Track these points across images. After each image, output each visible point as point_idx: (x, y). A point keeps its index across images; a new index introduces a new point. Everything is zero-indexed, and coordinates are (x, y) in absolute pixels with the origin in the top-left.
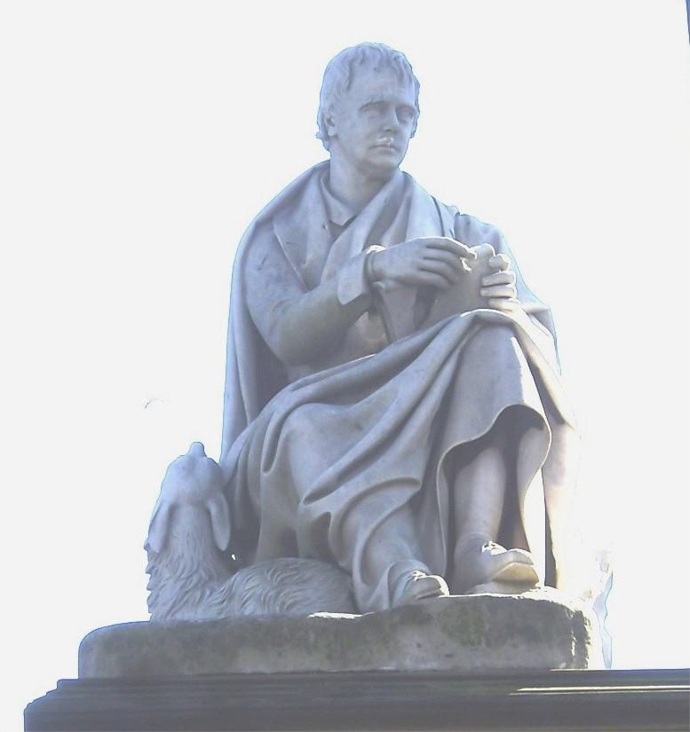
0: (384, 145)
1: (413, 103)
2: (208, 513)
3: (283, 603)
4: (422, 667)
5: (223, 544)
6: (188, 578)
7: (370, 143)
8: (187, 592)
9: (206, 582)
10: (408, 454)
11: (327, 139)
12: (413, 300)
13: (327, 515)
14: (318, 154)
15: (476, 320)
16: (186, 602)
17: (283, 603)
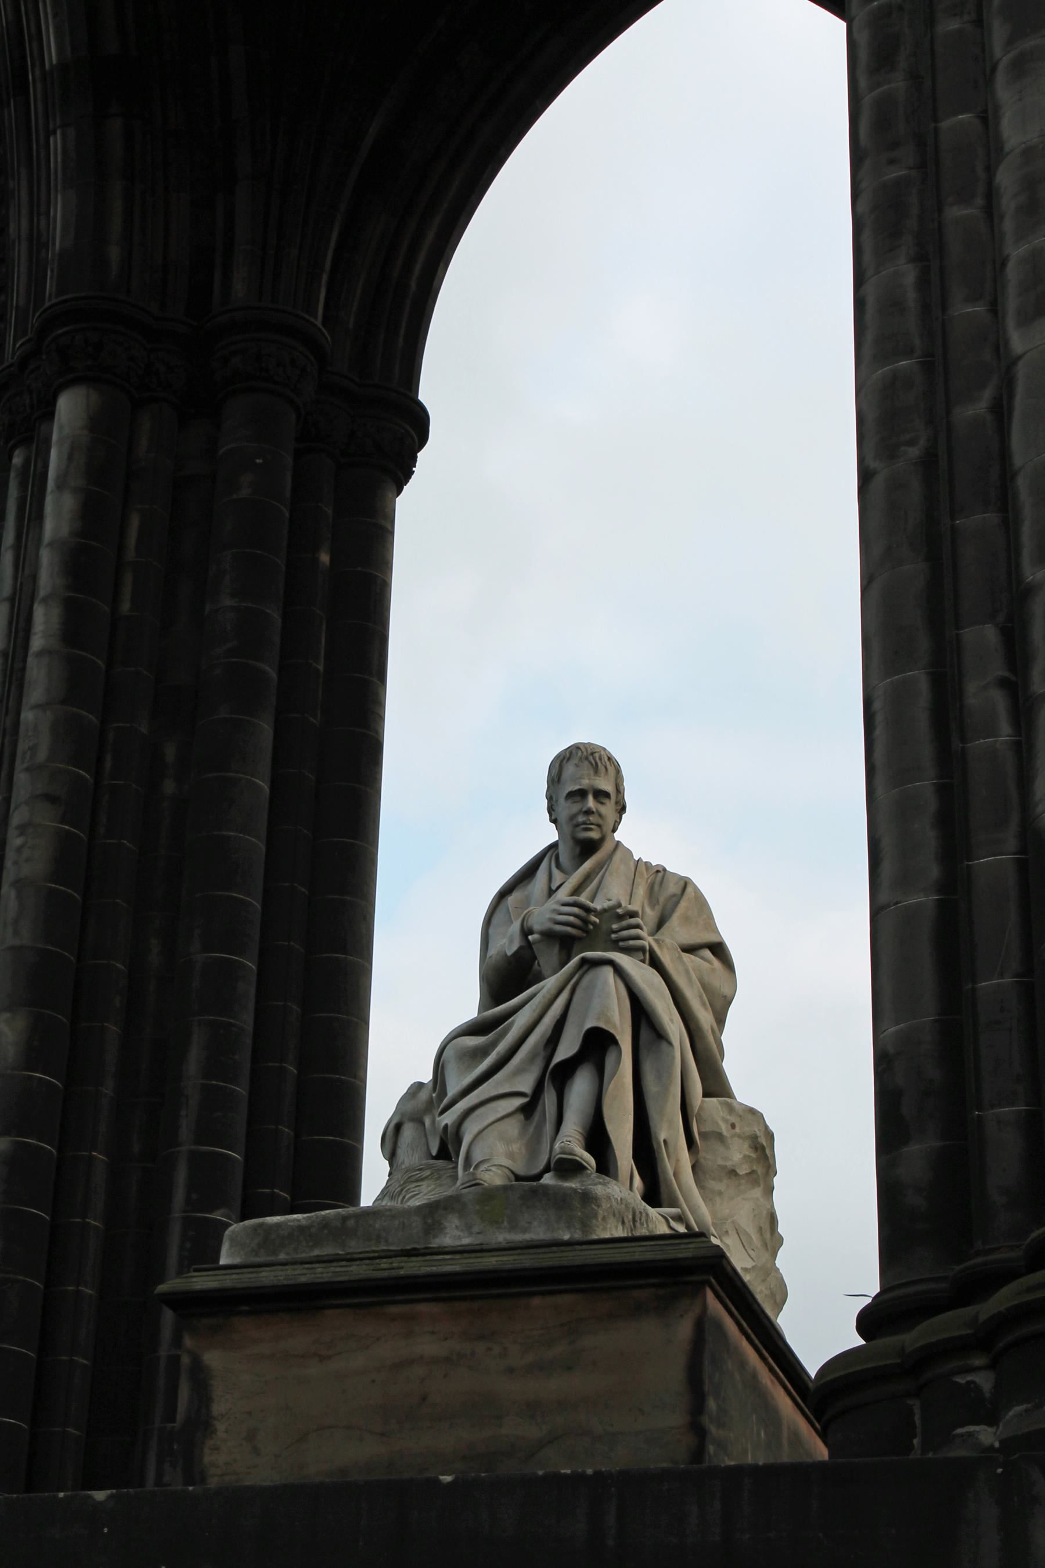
0: (584, 823)
1: (607, 786)
4: (458, 1243)
5: (434, 1152)
7: (574, 822)
11: (554, 821)
12: (556, 949)
13: (446, 1125)
14: (550, 834)
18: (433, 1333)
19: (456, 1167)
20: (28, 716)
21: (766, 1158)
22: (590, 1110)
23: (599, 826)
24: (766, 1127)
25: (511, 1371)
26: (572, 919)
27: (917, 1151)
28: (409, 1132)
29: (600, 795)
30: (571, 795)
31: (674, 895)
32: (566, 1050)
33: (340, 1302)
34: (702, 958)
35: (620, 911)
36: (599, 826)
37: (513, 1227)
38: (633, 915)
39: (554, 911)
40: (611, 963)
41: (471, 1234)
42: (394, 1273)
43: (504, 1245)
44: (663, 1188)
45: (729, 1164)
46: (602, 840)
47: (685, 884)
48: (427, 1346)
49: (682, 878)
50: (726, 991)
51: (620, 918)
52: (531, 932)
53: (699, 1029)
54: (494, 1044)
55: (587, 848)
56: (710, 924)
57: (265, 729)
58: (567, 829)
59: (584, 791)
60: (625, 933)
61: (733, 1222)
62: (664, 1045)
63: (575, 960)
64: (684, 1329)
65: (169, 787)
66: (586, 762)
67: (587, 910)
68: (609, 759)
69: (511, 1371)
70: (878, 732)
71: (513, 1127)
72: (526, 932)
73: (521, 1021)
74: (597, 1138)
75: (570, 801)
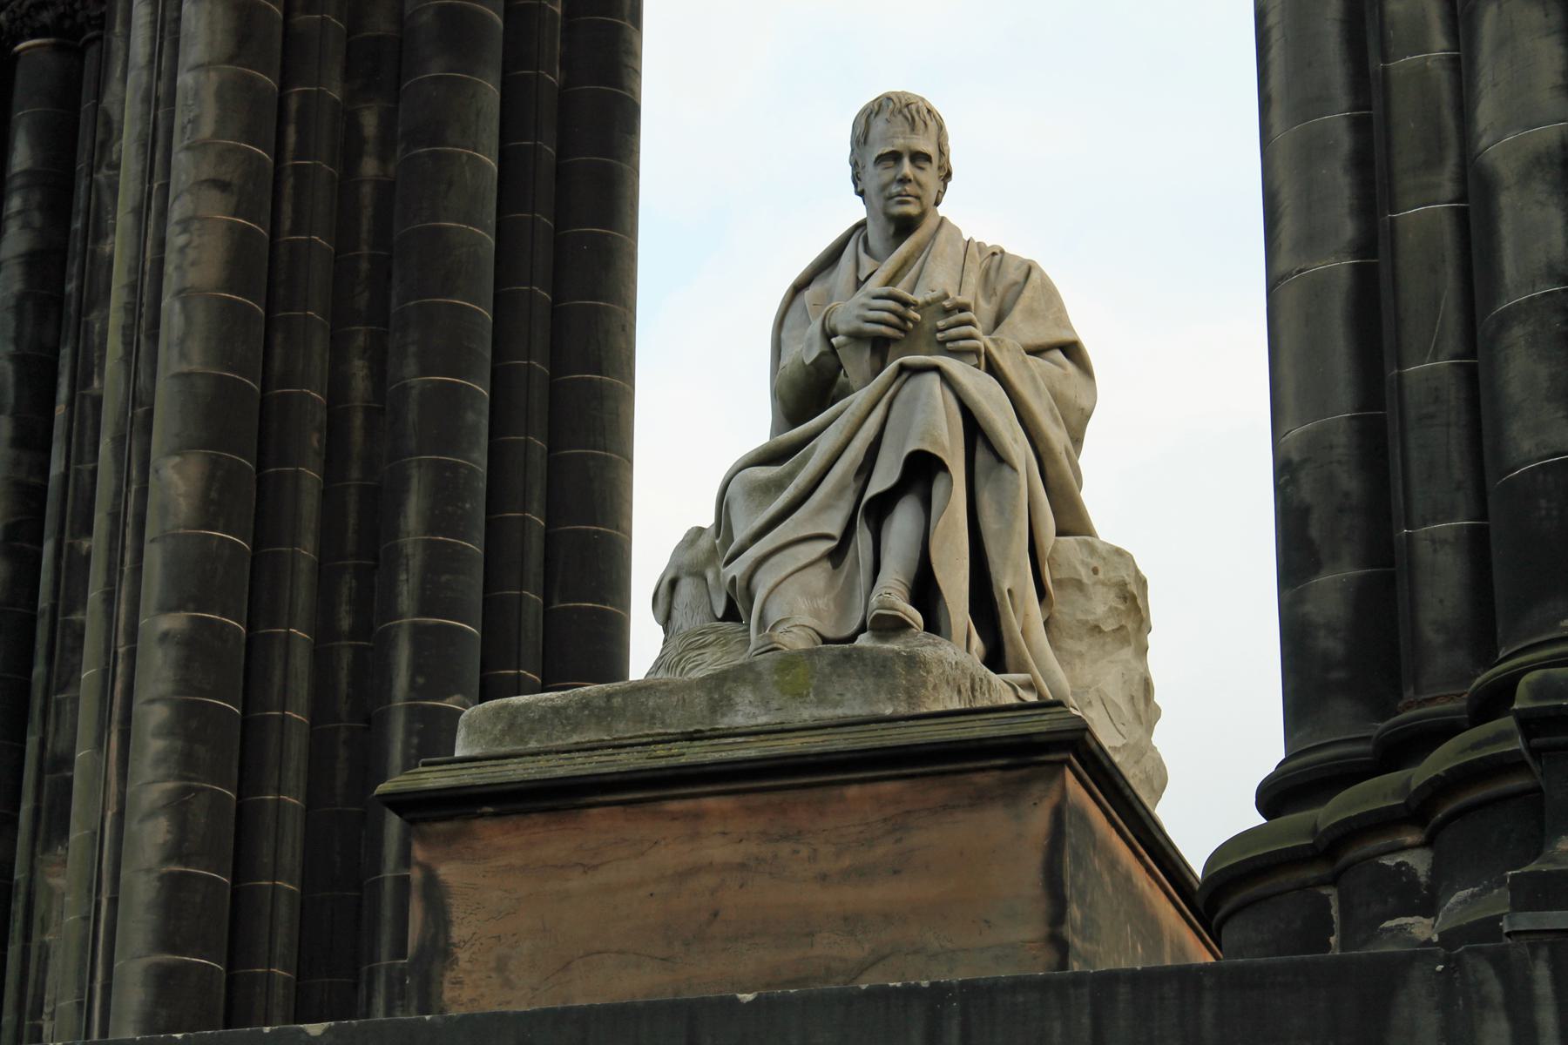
1: (929, 148)
4: (753, 722)
5: (719, 615)
7: (887, 193)
10: (825, 507)
11: (861, 193)
12: (867, 354)
13: (734, 579)
14: (857, 211)
15: (903, 368)
18: (724, 833)
19: (748, 630)
20: (185, 79)
21: (1137, 610)
22: (915, 555)
23: (918, 197)
24: (1137, 572)
25: (823, 878)
26: (886, 315)
27: (1333, 584)
28: (686, 588)
29: (919, 158)
30: (881, 159)
31: (1016, 283)
32: (884, 477)
34: (1053, 362)
35: (946, 304)
36: (918, 197)
37: (821, 702)
38: (963, 308)
39: (863, 305)
40: (936, 368)
41: (768, 711)
42: (673, 762)
43: (810, 723)
44: (1008, 649)
45: (1090, 618)
46: (923, 215)
47: (1029, 269)
48: (717, 850)
49: (1023, 261)
50: (1084, 402)
51: (947, 312)
53: (1051, 450)
54: (791, 475)
55: (904, 227)
56: (1062, 319)
57: (490, 91)
58: (878, 203)
59: (898, 155)
60: (954, 332)
61: (1098, 690)
62: (1006, 470)
63: (892, 367)
64: (1039, 821)
65: (369, 167)
66: (900, 117)
67: (906, 303)
68: (929, 111)
69: (823, 878)
70: (1275, 53)
71: (818, 577)
72: (828, 334)
73: (823, 446)
74: (925, 590)
75: (880, 168)
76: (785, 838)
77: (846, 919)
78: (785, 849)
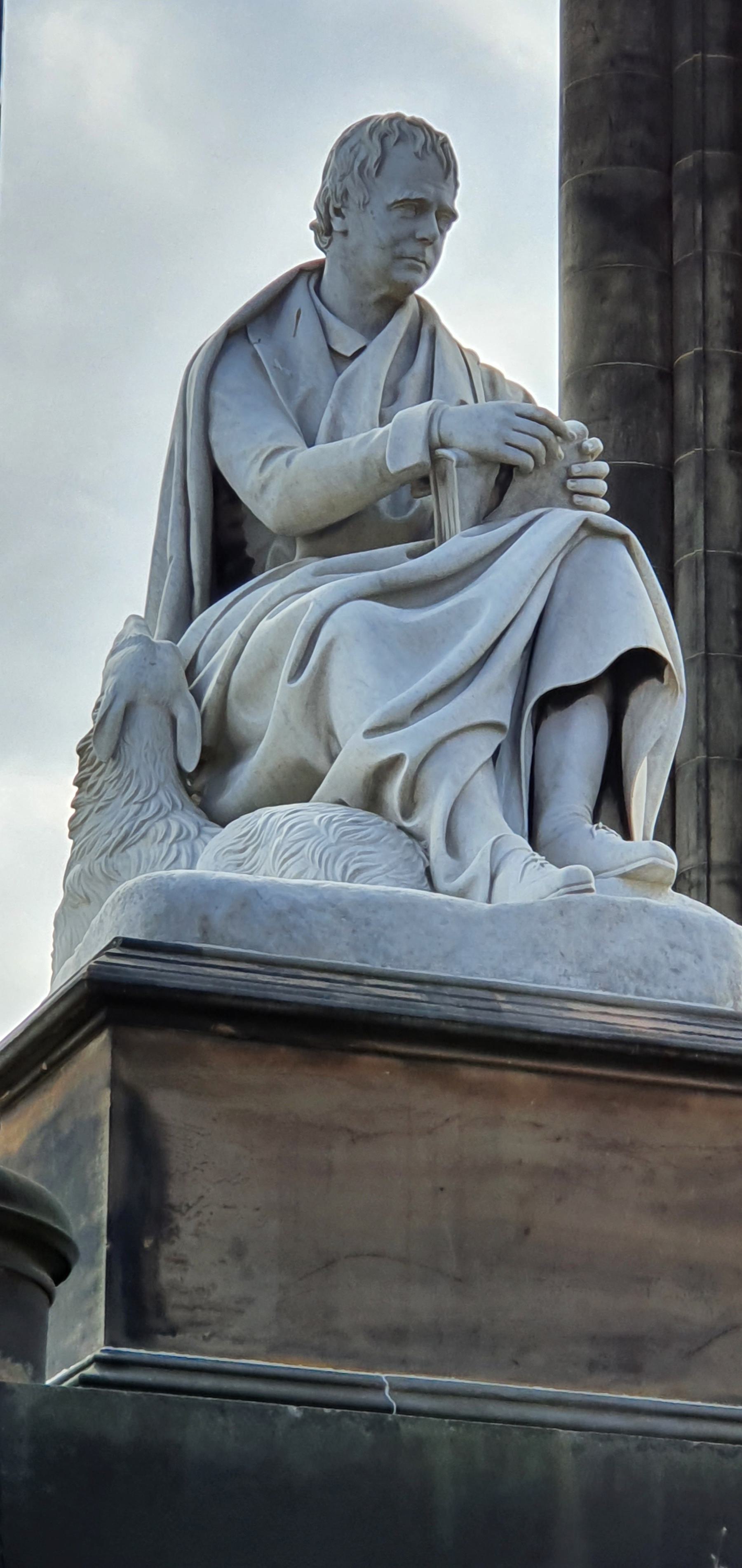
2: (173, 721)
3: (345, 868)
5: (190, 766)
6: (143, 803)
7: (398, 250)
8: (144, 822)
9: (168, 812)
11: (324, 231)
16: (144, 835)
17: (345, 868)
18: (537, 1126)
25: (661, 1209)
28: (148, 722)
33: (381, 1046)
52: (443, 446)
76: (615, 1146)
77: (691, 1268)
78: (615, 1160)
